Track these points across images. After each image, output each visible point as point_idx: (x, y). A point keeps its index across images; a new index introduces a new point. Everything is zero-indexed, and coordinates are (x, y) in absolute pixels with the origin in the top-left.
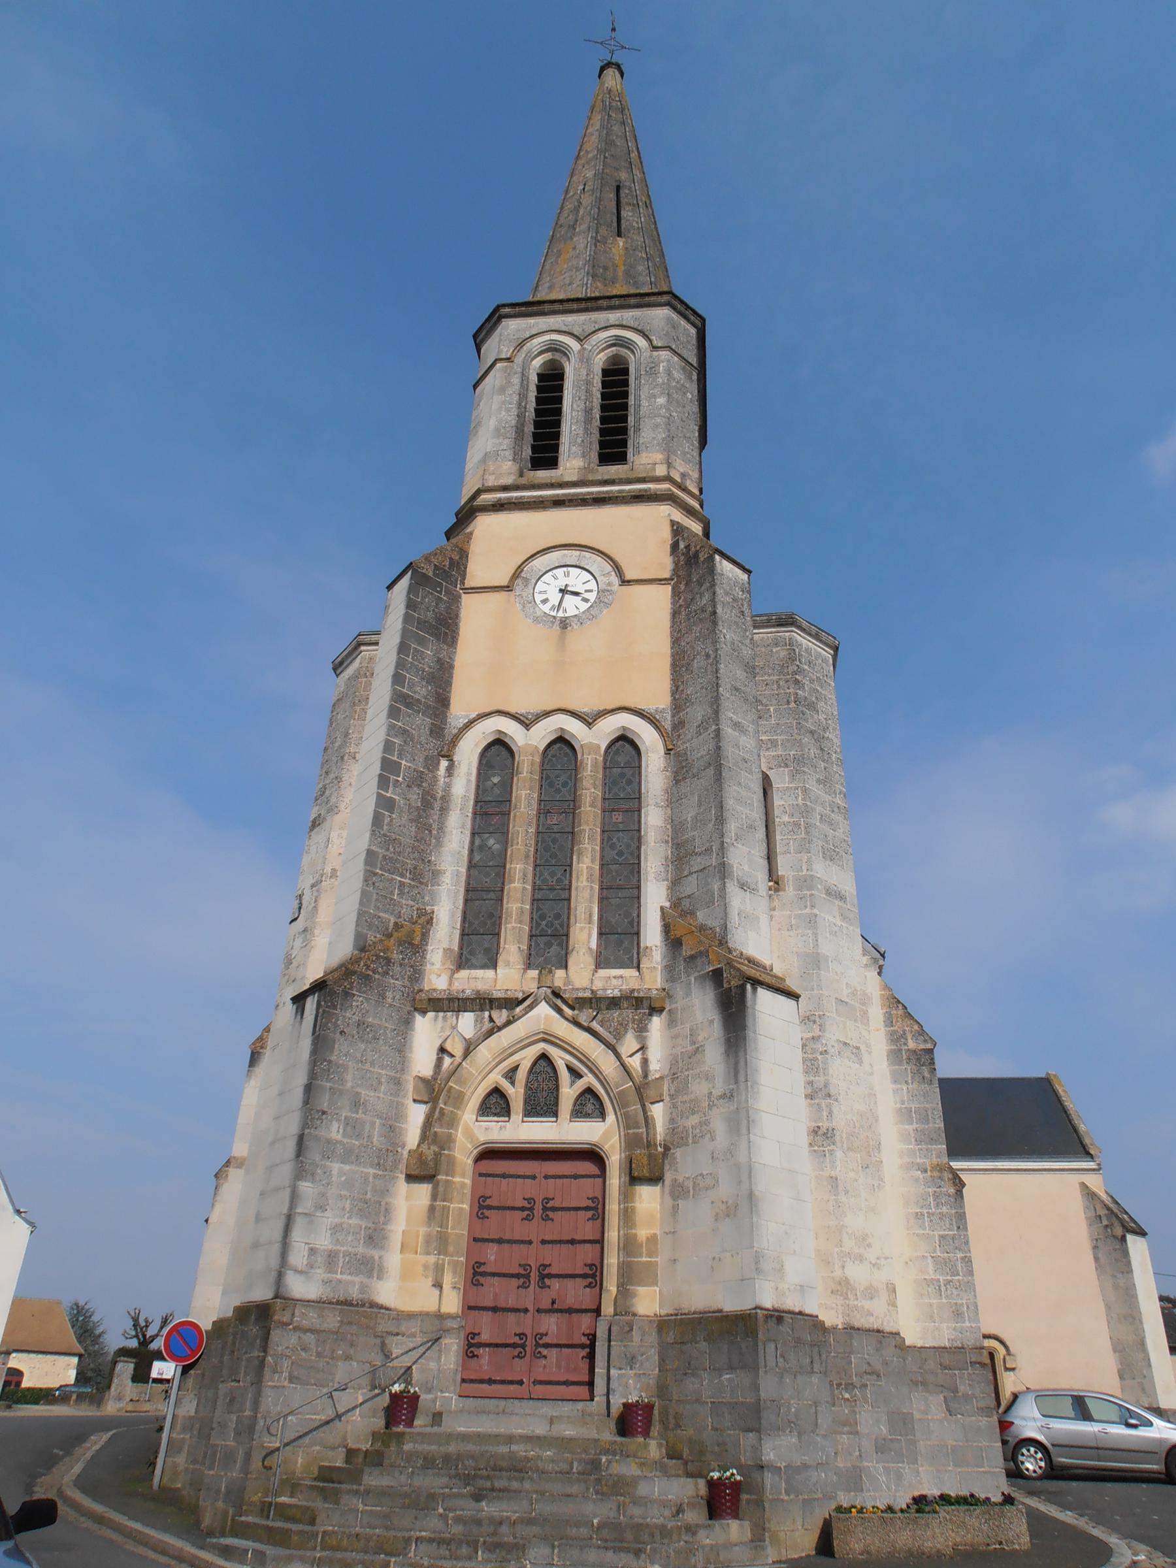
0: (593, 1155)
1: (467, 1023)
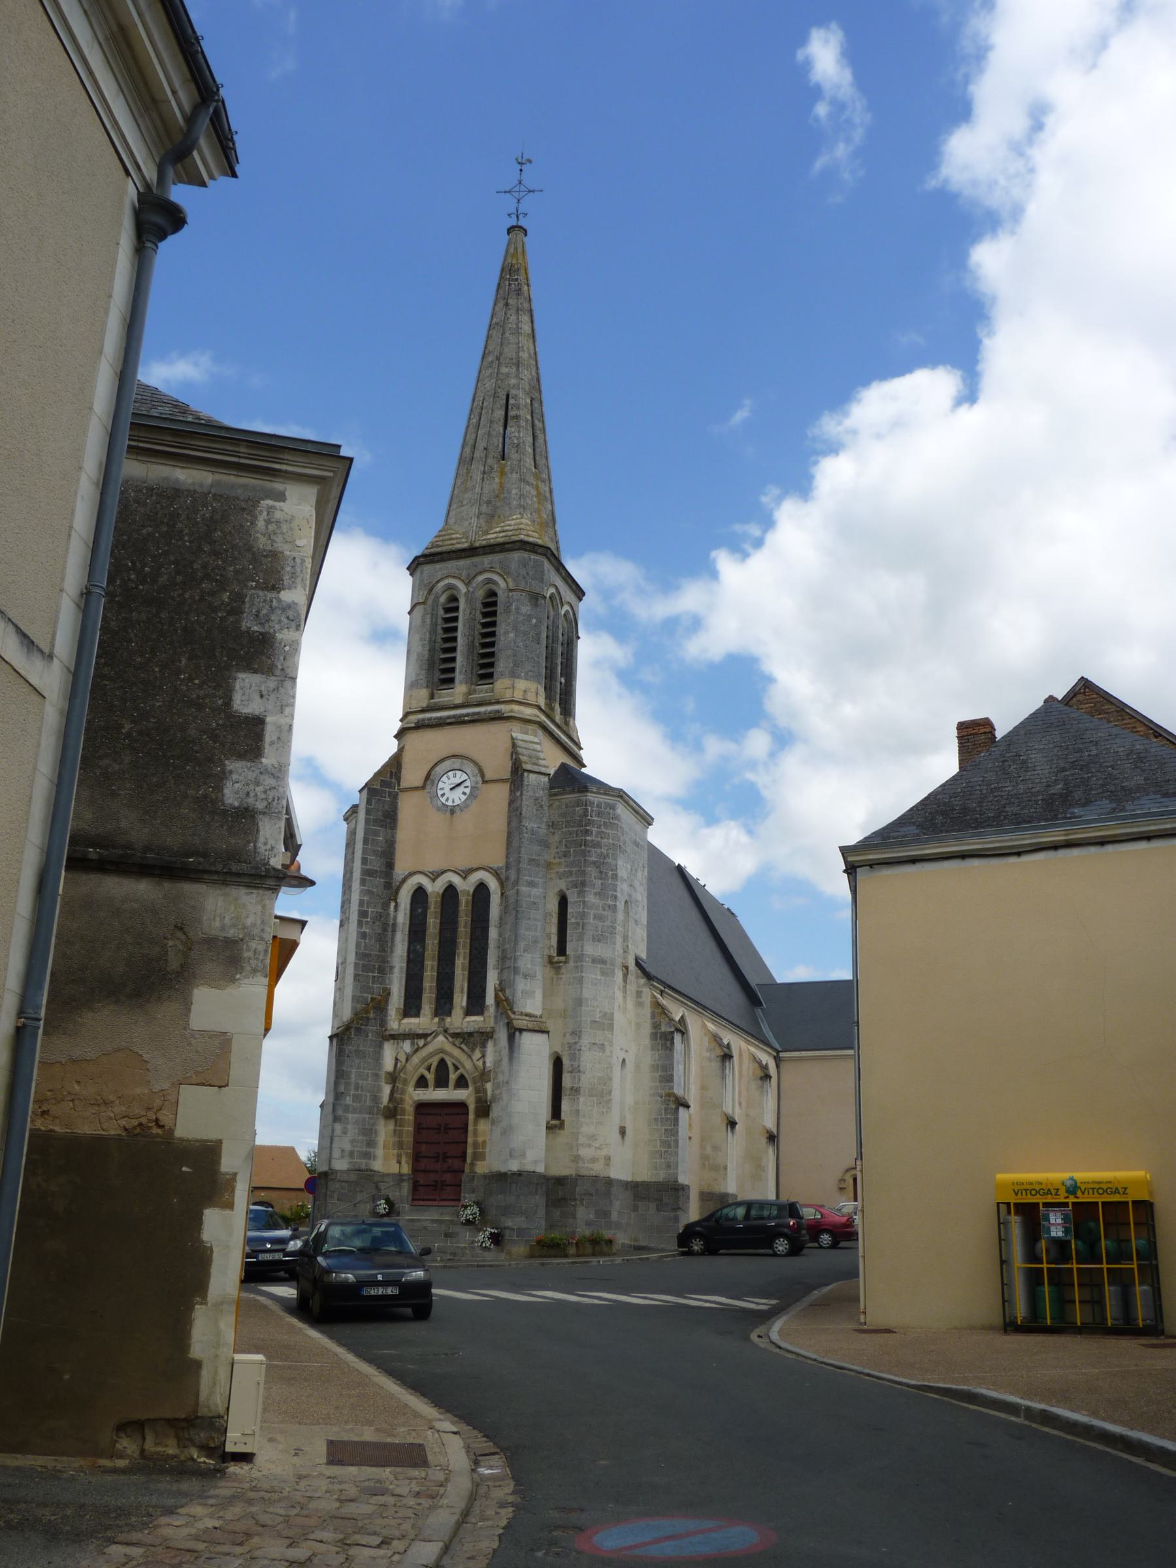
0: (462, 1106)
1: (407, 1046)
